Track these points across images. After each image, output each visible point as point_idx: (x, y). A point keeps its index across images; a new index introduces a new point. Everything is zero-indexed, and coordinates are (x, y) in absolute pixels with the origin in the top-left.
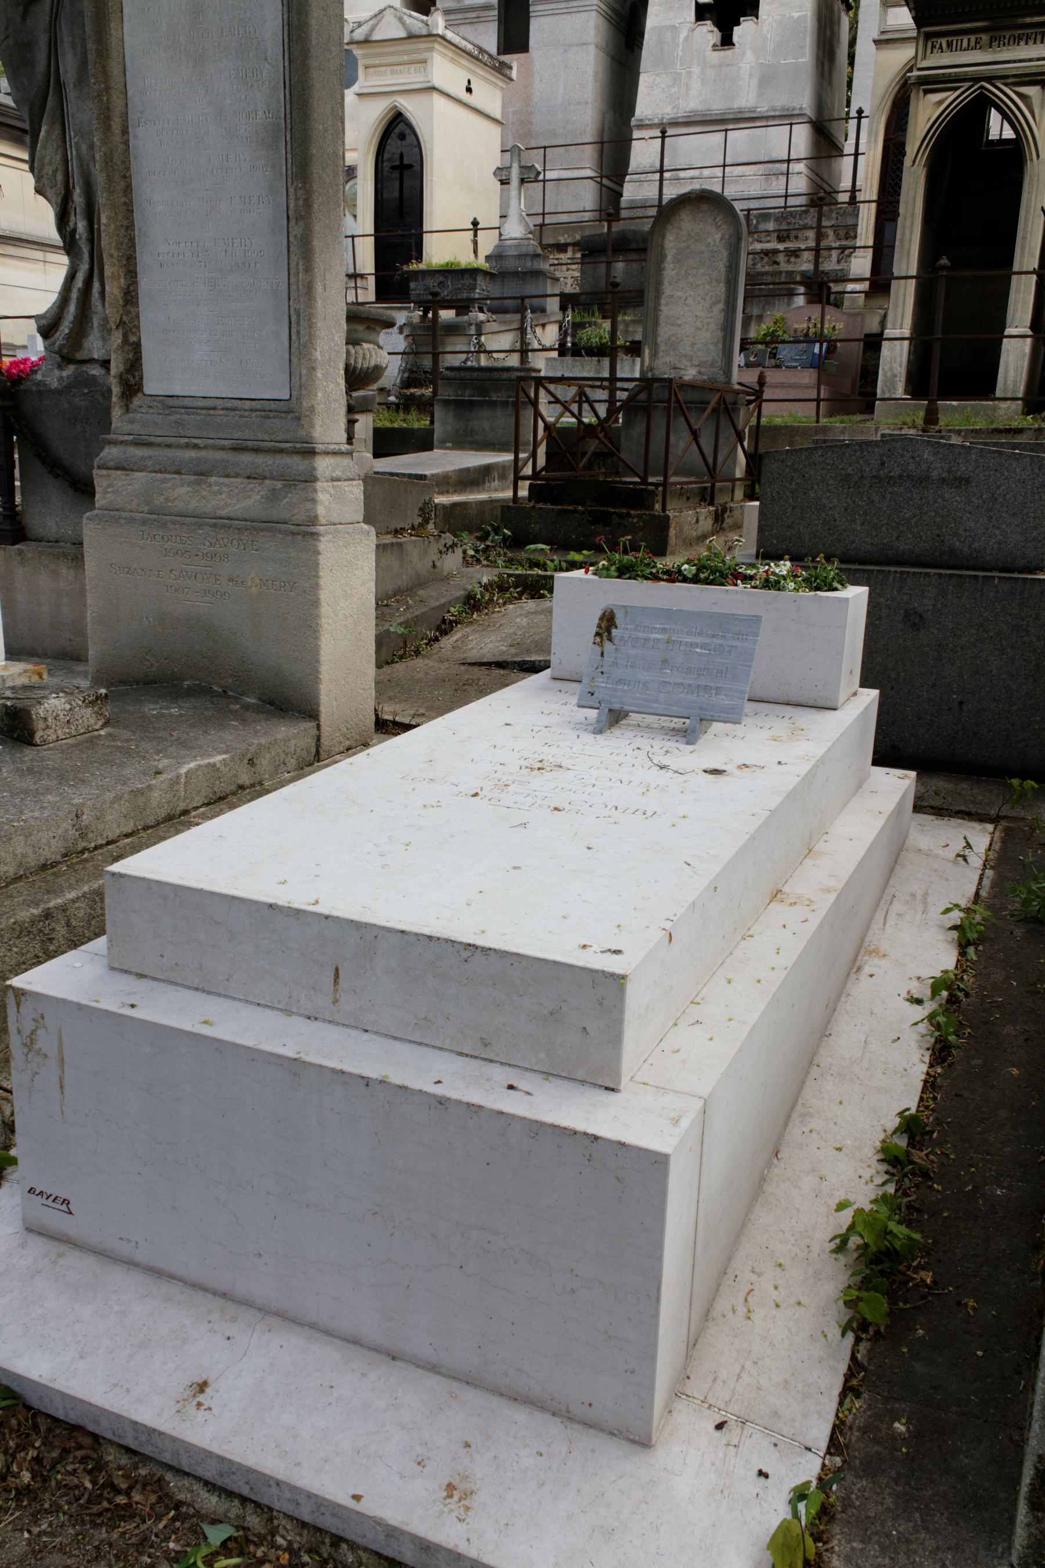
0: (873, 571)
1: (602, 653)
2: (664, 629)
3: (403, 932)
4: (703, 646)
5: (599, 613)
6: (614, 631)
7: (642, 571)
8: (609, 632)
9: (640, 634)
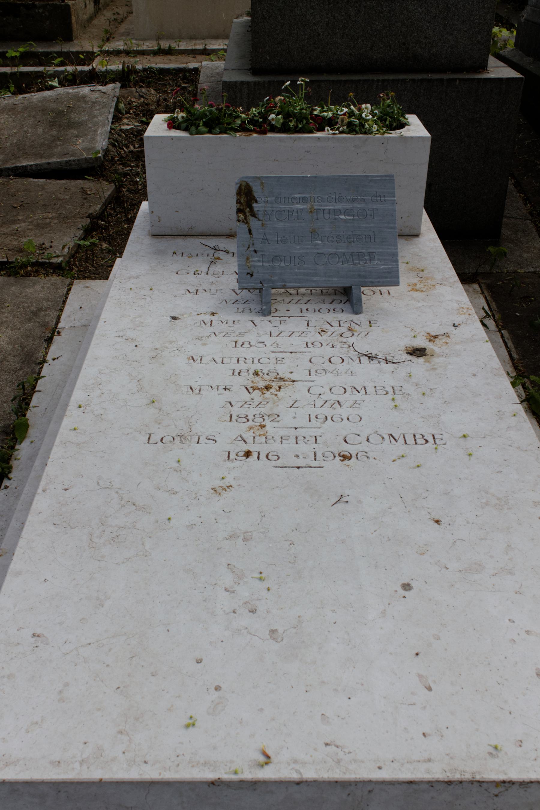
0: (360, 80)
1: (250, 232)
2: (304, 198)
3: (411, 783)
4: (346, 212)
5: (234, 190)
6: (255, 205)
7: (229, 124)
8: (251, 208)
9: (282, 207)
